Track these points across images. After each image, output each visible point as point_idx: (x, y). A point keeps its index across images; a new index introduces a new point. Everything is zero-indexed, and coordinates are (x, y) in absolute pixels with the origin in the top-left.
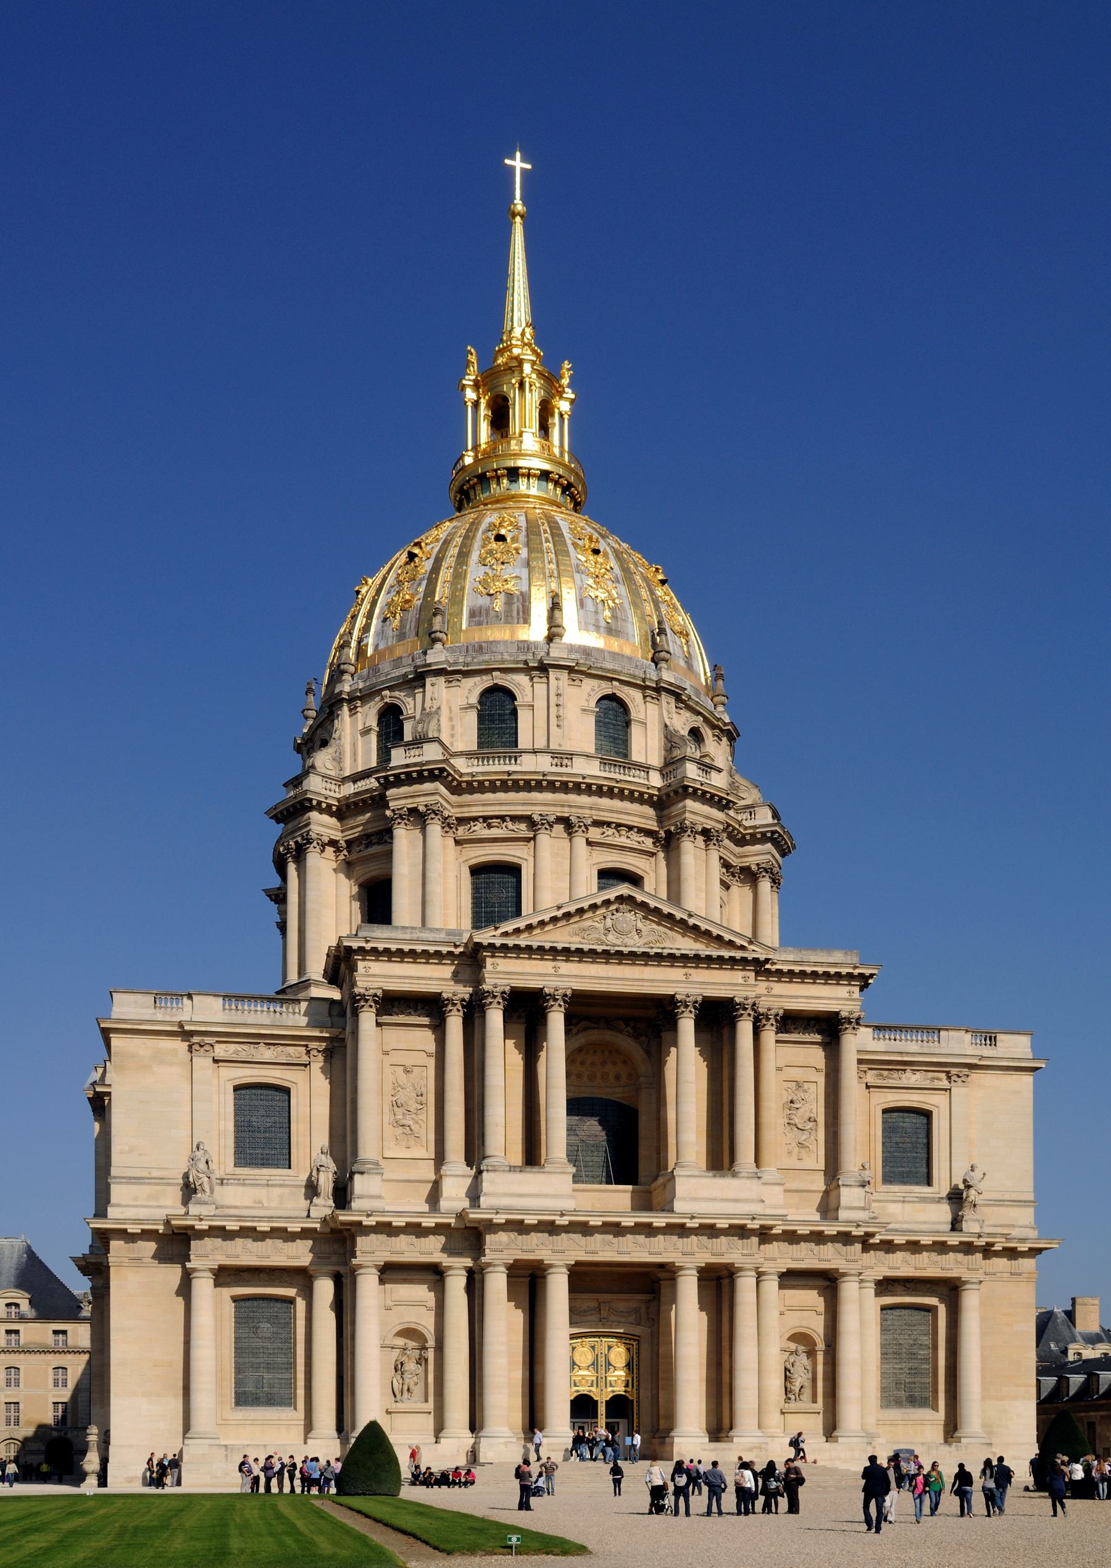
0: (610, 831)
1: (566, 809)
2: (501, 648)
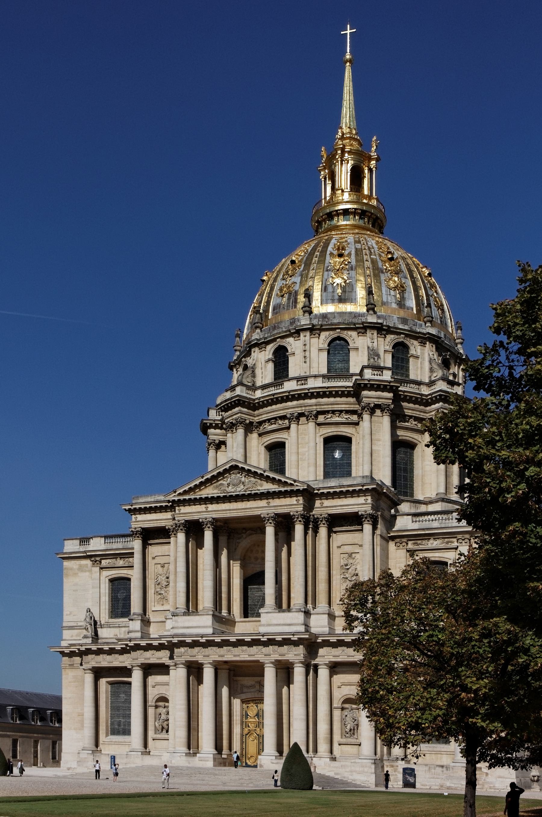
0: (330, 416)
1: (303, 408)
2: (283, 324)
